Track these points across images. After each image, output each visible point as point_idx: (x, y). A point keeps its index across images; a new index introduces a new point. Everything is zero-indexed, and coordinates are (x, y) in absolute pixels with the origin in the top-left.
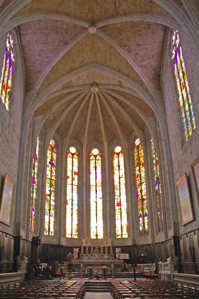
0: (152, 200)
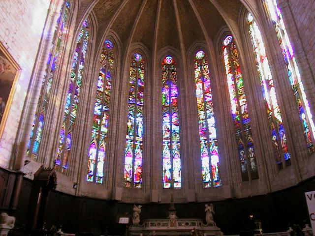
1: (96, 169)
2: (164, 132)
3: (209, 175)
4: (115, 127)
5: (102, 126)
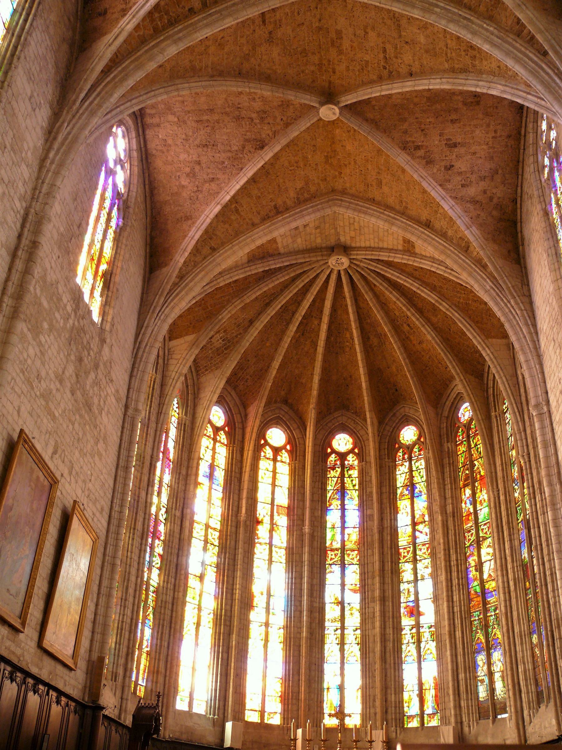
0: (513, 595)
3: (416, 702)
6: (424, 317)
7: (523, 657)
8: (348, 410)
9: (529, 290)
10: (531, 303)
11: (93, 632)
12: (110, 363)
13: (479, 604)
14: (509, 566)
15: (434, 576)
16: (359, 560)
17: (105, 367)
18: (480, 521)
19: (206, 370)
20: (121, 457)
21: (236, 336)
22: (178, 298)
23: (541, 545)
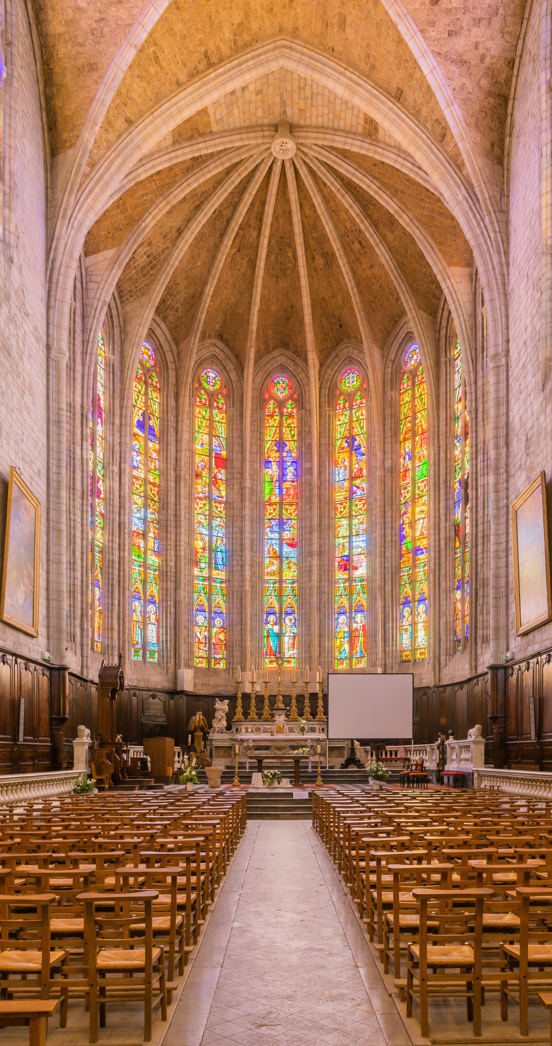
0: (443, 553)
1: (144, 638)
2: (267, 561)
4: (173, 553)
5: (149, 552)
6: (379, 233)
7: (446, 611)
8: (288, 348)
9: (508, 204)
10: (507, 222)
11: (48, 599)
12: (23, 291)
13: (409, 561)
14: (442, 525)
15: (369, 532)
16: (297, 515)
17: (18, 297)
18: (417, 478)
19: (131, 296)
20: (51, 410)
21: (163, 251)
22: (91, 197)
23: (477, 507)
